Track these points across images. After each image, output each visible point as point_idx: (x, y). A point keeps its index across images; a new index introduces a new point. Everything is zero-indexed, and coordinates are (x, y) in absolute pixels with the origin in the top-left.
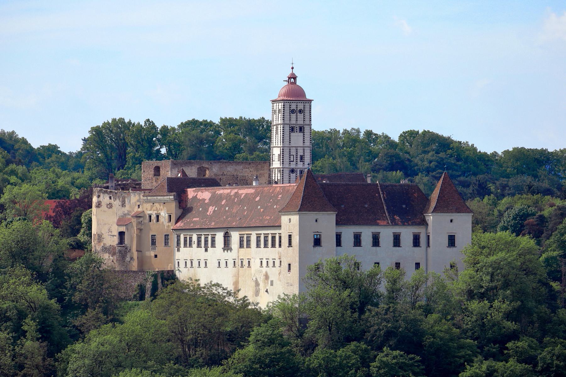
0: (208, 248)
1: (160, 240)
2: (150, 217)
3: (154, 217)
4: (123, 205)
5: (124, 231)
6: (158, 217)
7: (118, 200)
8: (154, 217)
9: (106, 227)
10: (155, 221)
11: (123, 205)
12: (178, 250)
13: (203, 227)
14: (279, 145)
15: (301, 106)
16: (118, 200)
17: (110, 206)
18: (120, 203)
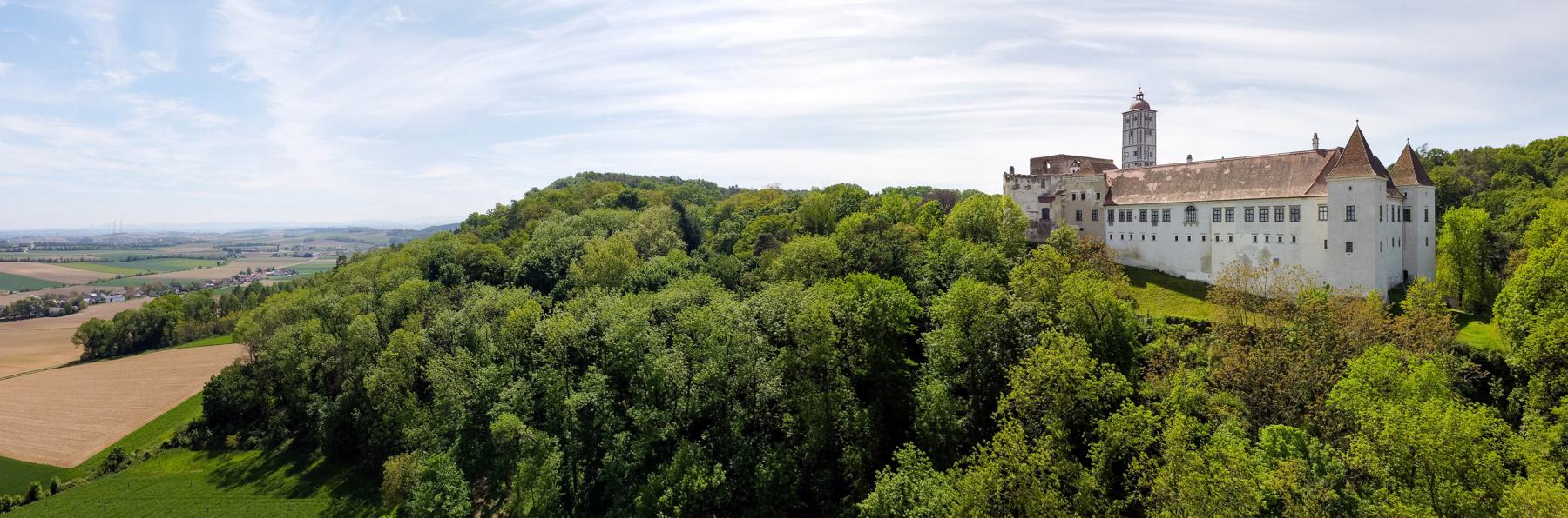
0: (1158, 223)
1: (1087, 215)
2: (1074, 196)
3: (1078, 195)
4: (1043, 186)
5: (1048, 207)
6: (1083, 196)
7: (1037, 183)
8: (1078, 195)
9: (1025, 205)
10: (1080, 199)
11: (1043, 186)
12: (1111, 224)
13: (1150, 202)
14: (1136, 144)
15: (1150, 116)
16: (1037, 183)
17: (1029, 188)
18: (1040, 185)
